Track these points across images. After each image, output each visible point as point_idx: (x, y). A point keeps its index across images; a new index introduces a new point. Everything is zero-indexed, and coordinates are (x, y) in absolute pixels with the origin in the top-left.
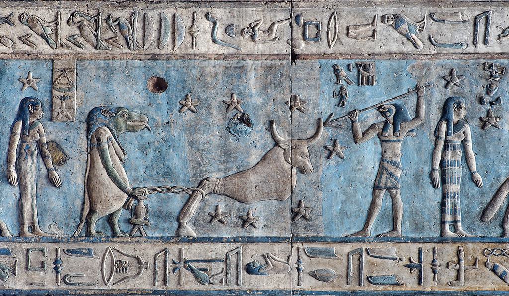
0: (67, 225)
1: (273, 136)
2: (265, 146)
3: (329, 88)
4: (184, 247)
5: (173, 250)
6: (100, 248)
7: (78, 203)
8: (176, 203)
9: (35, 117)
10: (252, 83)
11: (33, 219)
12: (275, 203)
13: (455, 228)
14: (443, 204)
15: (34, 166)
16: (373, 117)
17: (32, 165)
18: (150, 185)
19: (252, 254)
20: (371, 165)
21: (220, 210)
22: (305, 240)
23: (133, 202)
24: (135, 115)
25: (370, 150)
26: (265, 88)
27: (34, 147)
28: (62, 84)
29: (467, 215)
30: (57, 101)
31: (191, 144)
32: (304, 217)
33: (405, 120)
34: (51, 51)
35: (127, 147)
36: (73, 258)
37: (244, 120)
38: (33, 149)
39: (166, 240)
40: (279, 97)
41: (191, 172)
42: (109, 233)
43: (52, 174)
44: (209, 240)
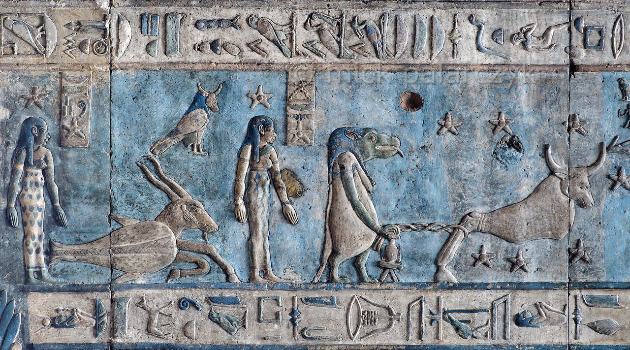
0: (305, 269)
1: (548, 163)
2: (538, 175)
4: (443, 295)
5: (430, 298)
6: (344, 296)
7: (318, 243)
8: (434, 243)
9: (266, 140)
10: (524, 99)
11: (265, 262)
12: (549, 242)
15: (265, 199)
17: (263, 198)
18: (404, 221)
19: (522, 302)
21: (486, 251)
22: (583, 286)
23: (383, 242)
24: (385, 138)
26: (538, 105)
27: (265, 176)
28: (298, 100)
30: (293, 121)
31: (452, 172)
32: (583, 259)
34: (285, 60)
35: (376, 176)
36: (312, 308)
37: (514, 144)
38: (264, 178)
39: (421, 287)
40: (555, 116)
41: (451, 206)
42: (355, 279)
43: (287, 209)
44: (472, 286)
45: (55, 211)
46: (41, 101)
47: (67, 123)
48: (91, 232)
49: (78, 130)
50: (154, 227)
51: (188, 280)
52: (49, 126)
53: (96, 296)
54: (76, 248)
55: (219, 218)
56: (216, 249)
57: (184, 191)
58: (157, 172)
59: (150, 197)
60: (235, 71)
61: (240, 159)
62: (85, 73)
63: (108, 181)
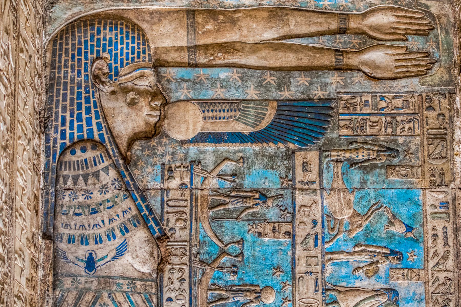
0: (332, 278)
9: (392, 259)
11: (335, 259)
15: (364, 259)
17: (365, 257)
27: (375, 259)
28: (411, 274)
30: (401, 272)
34: (430, 268)
38: (374, 259)
43: (360, 270)
45: (357, 163)
46: (407, 157)
47: (397, 169)
48: (347, 180)
49: (394, 174)
50: (350, 208)
51: (326, 224)
52: (396, 161)
53: (318, 183)
54: (340, 173)
55: (355, 238)
57: (367, 222)
58: (376, 210)
59: (364, 206)
60: (424, 245)
61: (382, 248)
62: (421, 177)
63: (371, 187)
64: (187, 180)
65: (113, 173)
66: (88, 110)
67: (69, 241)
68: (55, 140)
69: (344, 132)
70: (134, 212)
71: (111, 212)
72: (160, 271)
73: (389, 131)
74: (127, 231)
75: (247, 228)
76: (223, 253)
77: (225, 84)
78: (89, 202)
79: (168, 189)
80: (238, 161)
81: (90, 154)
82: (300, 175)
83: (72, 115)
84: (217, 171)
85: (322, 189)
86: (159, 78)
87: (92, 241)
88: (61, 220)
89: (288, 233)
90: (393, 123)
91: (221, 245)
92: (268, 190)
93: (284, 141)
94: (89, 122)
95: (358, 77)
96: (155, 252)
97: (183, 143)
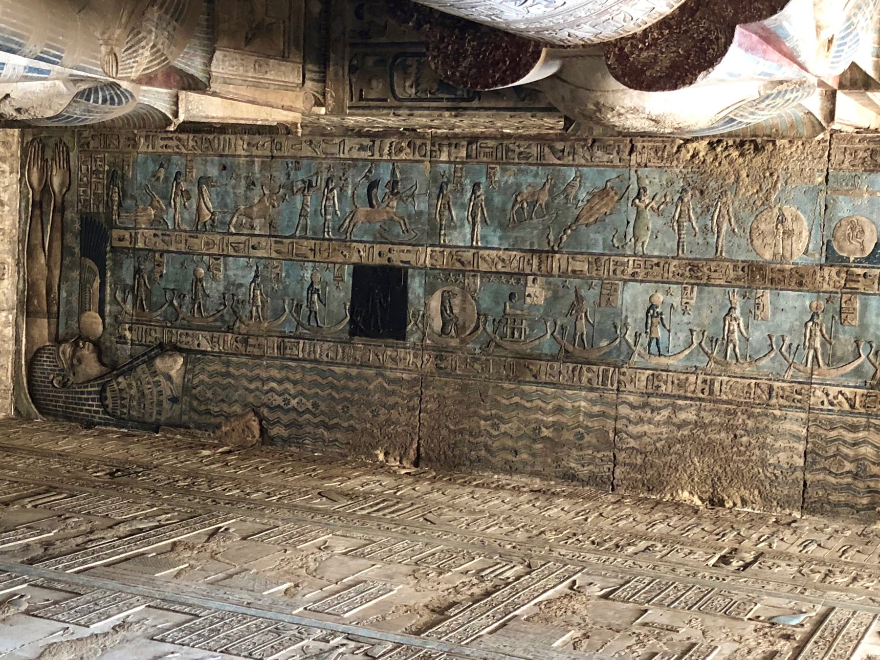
3: (284, 172)
5: (226, 237)
8: (228, 219)
10: (257, 168)
13: (328, 234)
14: (325, 224)
16: (300, 185)
19: (254, 241)
20: (299, 206)
25: (299, 198)
27: (180, 193)
29: (333, 229)
33: (312, 186)
37: (253, 184)
56: (165, 217)
64: (127, 326)
65: (120, 379)
66: (82, 393)
67: (160, 414)
68: (100, 418)
69: (101, 209)
70: (144, 366)
71: (144, 383)
72: (181, 351)
73: (101, 176)
74: (156, 372)
75: (157, 285)
76: (171, 304)
77: (70, 294)
78: (137, 398)
79: (132, 340)
80: (117, 288)
81: (109, 394)
82: (126, 244)
83: (85, 405)
84: (122, 304)
85: (135, 228)
86: (66, 341)
87: (161, 398)
88: (147, 418)
89: (161, 256)
90: (96, 172)
91: (166, 305)
92: (134, 267)
93: (106, 253)
94: (89, 393)
95: (68, 197)
96: (170, 353)
97: (104, 327)
